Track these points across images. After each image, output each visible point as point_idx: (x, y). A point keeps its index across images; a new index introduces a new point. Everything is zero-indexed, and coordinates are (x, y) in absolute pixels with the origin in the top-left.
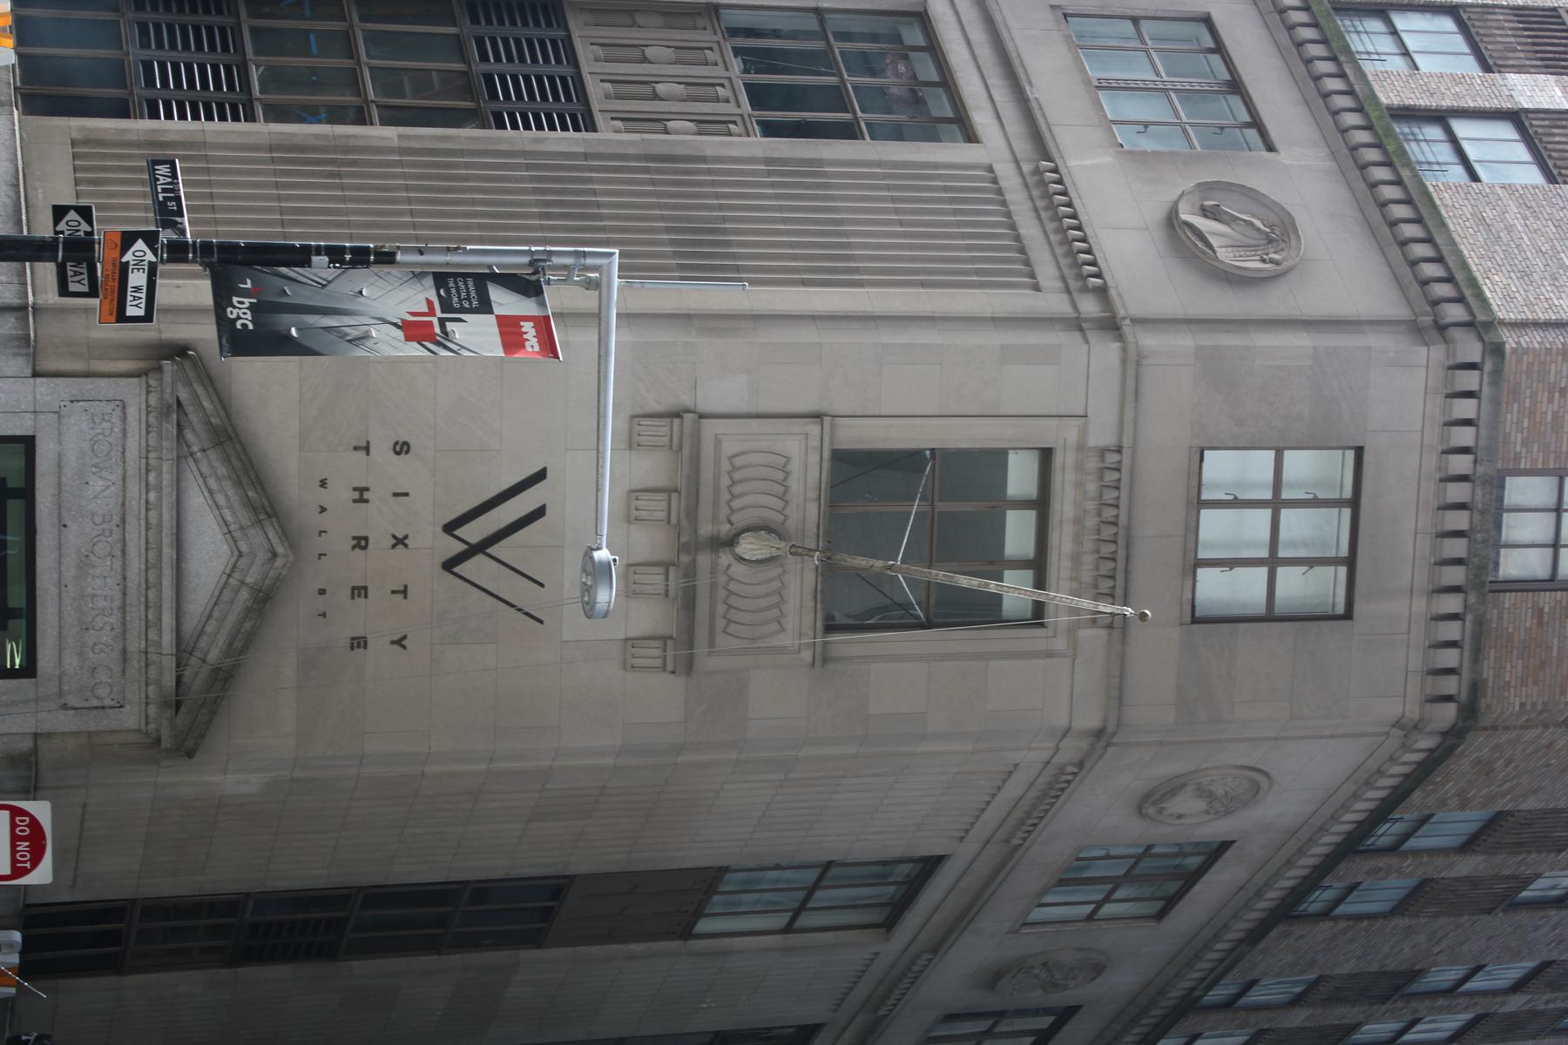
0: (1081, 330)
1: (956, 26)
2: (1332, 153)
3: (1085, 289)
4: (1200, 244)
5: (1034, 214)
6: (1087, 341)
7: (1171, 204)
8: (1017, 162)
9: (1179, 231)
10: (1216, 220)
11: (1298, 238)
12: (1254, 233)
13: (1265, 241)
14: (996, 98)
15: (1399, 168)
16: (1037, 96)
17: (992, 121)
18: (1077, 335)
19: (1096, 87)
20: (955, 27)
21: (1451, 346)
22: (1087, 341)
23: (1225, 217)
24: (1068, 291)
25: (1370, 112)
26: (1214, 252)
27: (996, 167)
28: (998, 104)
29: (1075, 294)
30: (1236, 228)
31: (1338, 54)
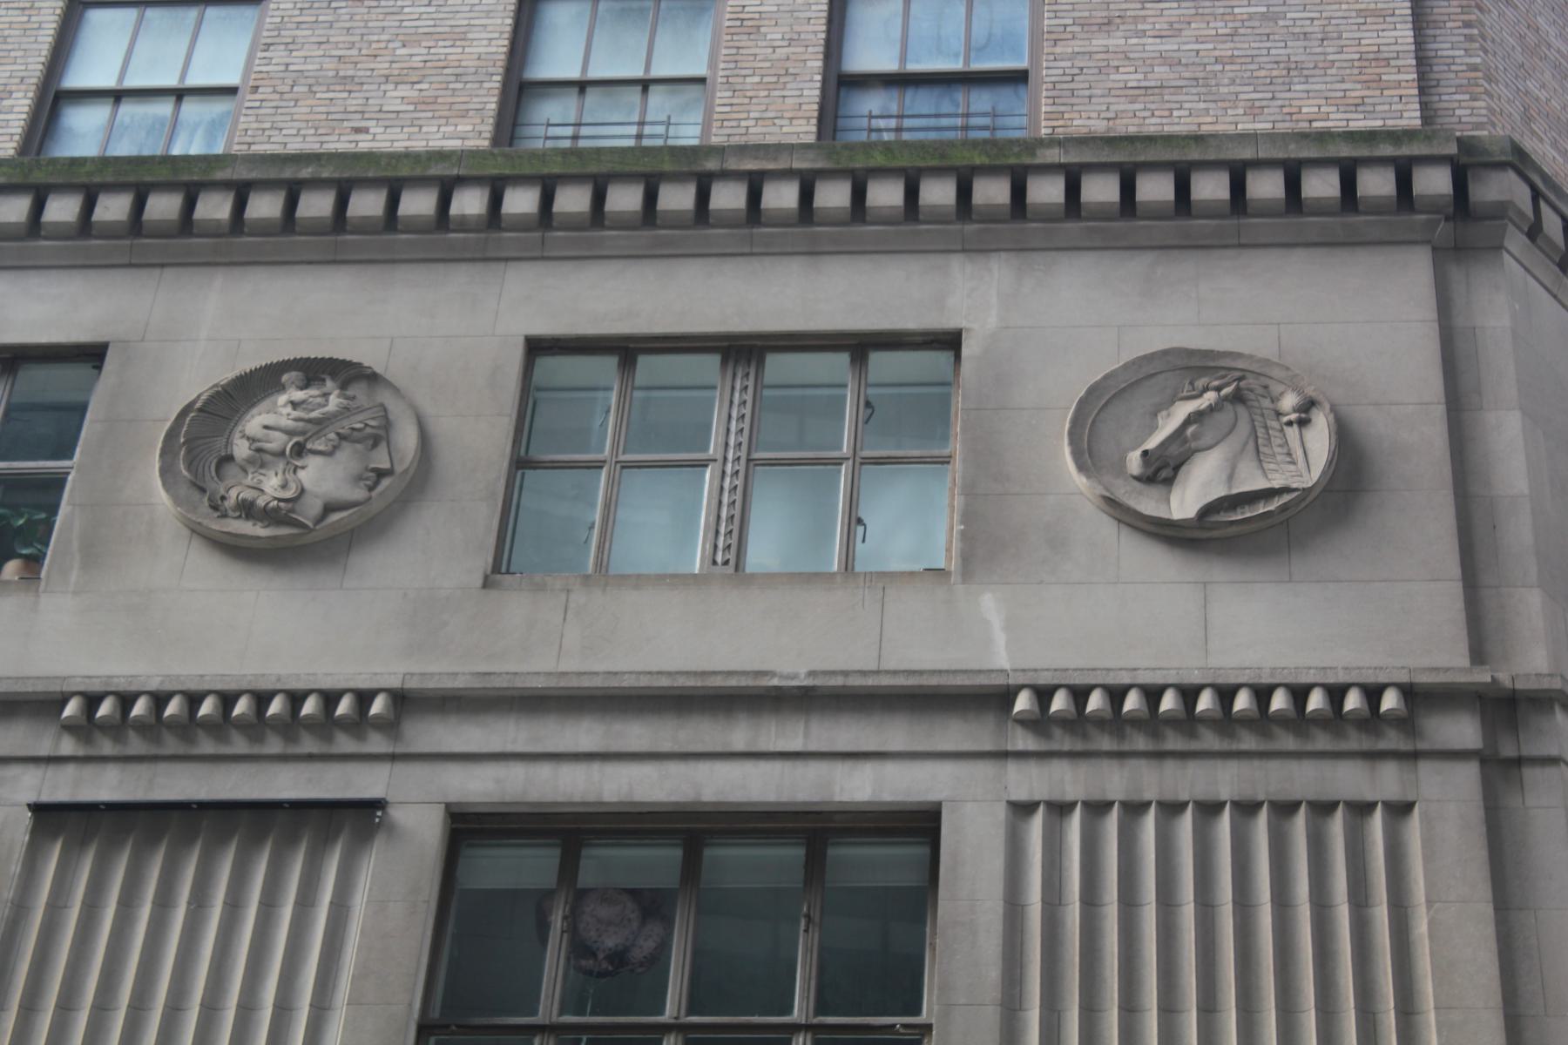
0: (1519, 762)
1: (596, 768)
2: (964, 251)
3: (1405, 723)
4: (1262, 508)
5: (1170, 766)
6: (1553, 761)
7: (1125, 531)
8: (1003, 755)
9: (1215, 534)
10: (1177, 469)
11: (1239, 355)
12: (1225, 417)
13: (1241, 409)
14: (796, 745)
15: (1038, 161)
16: (803, 671)
17: (868, 769)
18: (1530, 774)
19: (737, 568)
20: (544, 771)
21: (1511, 214)
22: (1553, 761)
23: (1174, 450)
24: (1414, 756)
25: (872, 163)
26: (1286, 490)
27: (1021, 795)
28: (813, 747)
29: (1422, 746)
30: (1207, 439)
31: (698, 168)
